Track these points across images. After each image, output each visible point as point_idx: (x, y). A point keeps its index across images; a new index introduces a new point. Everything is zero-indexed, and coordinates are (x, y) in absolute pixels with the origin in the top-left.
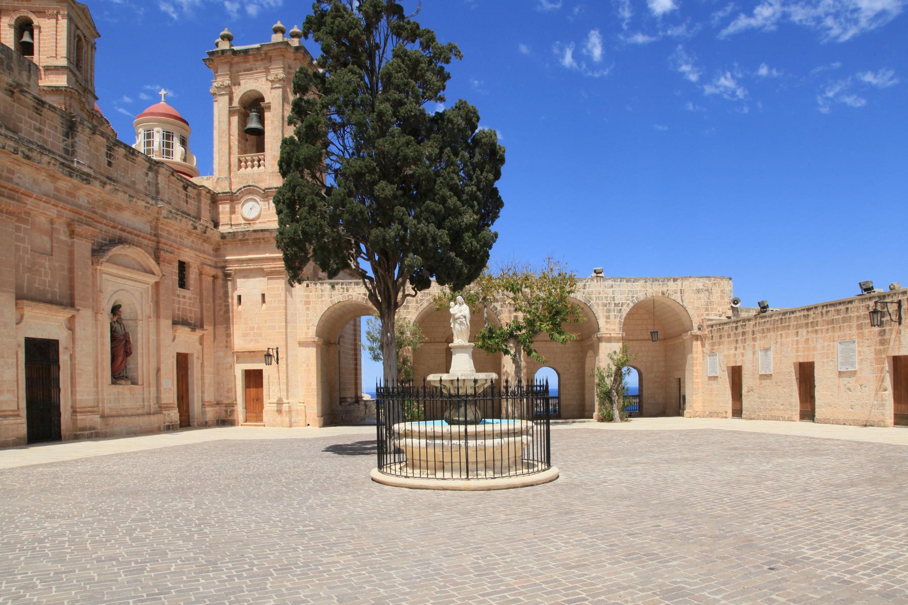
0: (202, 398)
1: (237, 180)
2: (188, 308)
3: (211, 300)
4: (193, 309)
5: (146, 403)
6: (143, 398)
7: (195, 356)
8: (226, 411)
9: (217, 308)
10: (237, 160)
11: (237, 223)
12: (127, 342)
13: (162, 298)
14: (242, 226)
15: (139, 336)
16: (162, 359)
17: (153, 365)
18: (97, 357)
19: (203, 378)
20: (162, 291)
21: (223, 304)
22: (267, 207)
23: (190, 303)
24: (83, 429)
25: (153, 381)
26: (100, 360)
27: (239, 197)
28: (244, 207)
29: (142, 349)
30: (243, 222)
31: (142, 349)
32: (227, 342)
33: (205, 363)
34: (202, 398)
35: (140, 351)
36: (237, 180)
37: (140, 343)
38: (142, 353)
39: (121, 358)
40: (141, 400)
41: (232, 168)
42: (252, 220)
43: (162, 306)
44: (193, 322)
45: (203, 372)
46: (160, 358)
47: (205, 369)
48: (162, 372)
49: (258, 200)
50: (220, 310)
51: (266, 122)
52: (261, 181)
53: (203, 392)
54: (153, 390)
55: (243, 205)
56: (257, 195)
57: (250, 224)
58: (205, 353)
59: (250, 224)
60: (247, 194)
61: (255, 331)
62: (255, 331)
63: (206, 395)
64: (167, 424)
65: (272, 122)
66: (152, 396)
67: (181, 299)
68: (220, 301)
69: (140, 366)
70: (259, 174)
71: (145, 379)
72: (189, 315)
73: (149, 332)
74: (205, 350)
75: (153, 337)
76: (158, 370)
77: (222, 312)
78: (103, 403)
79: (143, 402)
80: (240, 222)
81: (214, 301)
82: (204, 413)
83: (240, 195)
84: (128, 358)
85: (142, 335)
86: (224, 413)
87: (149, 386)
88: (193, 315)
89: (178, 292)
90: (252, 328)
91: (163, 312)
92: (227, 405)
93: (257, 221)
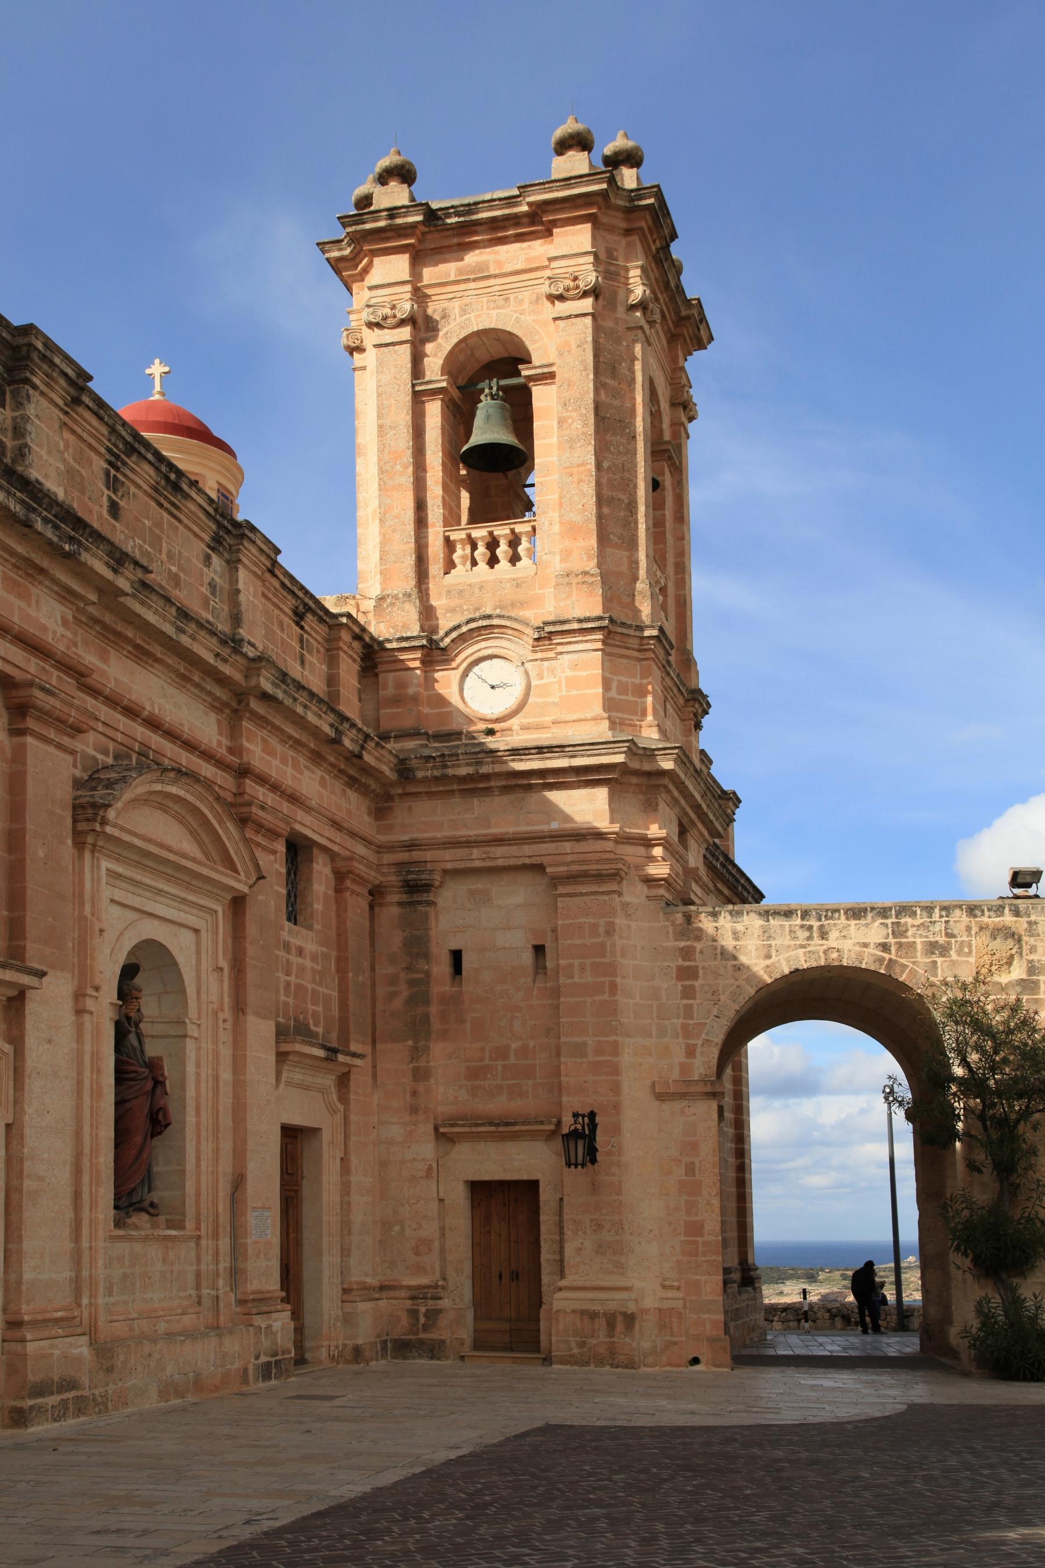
0: (344, 1270)
2: (310, 986)
3: (366, 964)
4: (322, 990)
5: (205, 1292)
6: (198, 1274)
7: (326, 1135)
8: (413, 1313)
9: (381, 991)
12: (158, 1083)
13: (251, 950)
15: (191, 1068)
16: (251, 1145)
17: (226, 1165)
18: (78, 1134)
19: (346, 1208)
20: (252, 930)
21: (403, 976)
23: (314, 971)
24: (41, 1390)
25: (224, 1218)
26: (87, 1150)
29: (198, 1114)
31: (198, 1114)
32: (414, 1093)
33: (354, 1160)
34: (344, 1270)
35: (190, 1118)
37: (191, 1092)
38: (198, 1124)
39: (138, 1139)
40: (191, 1278)
43: (251, 976)
44: (320, 1030)
45: (346, 1189)
46: (244, 1142)
47: (353, 1179)
48: (251, 1187)
50: (392, 996)
51: (537, 425)
52: (523, 604)
53: (345, 1252)
54: (224, 1244)
58: (353, 1128)
61: (512, 1060)
62: (512, 1060)
63: (353, 1261)
64: (263, 1359)
65: (561, 422)
66: (221, 1267)
67: (294, 959)
68: (390, 970)
69: (190, 1166)
70: (518, 584)
71: (204, 1211)
72: (311, 1007)
73: (216, 1054)
74: (353, 1118)
75: (226, 1075)
76: (238, 1182)
77: (398, 1003)
78: (93, 1296)
79: (198, 1286)
81: (373, 969)
82: (348, 1319)
84: (156, 1142)
85: (198, 1065)
86: (405, 1320)
87: (216, 1236)
88: (320, 1009)
89: (285, 935)
90: (502, 1053)
91: (253, 997)
92: (418, 1294)
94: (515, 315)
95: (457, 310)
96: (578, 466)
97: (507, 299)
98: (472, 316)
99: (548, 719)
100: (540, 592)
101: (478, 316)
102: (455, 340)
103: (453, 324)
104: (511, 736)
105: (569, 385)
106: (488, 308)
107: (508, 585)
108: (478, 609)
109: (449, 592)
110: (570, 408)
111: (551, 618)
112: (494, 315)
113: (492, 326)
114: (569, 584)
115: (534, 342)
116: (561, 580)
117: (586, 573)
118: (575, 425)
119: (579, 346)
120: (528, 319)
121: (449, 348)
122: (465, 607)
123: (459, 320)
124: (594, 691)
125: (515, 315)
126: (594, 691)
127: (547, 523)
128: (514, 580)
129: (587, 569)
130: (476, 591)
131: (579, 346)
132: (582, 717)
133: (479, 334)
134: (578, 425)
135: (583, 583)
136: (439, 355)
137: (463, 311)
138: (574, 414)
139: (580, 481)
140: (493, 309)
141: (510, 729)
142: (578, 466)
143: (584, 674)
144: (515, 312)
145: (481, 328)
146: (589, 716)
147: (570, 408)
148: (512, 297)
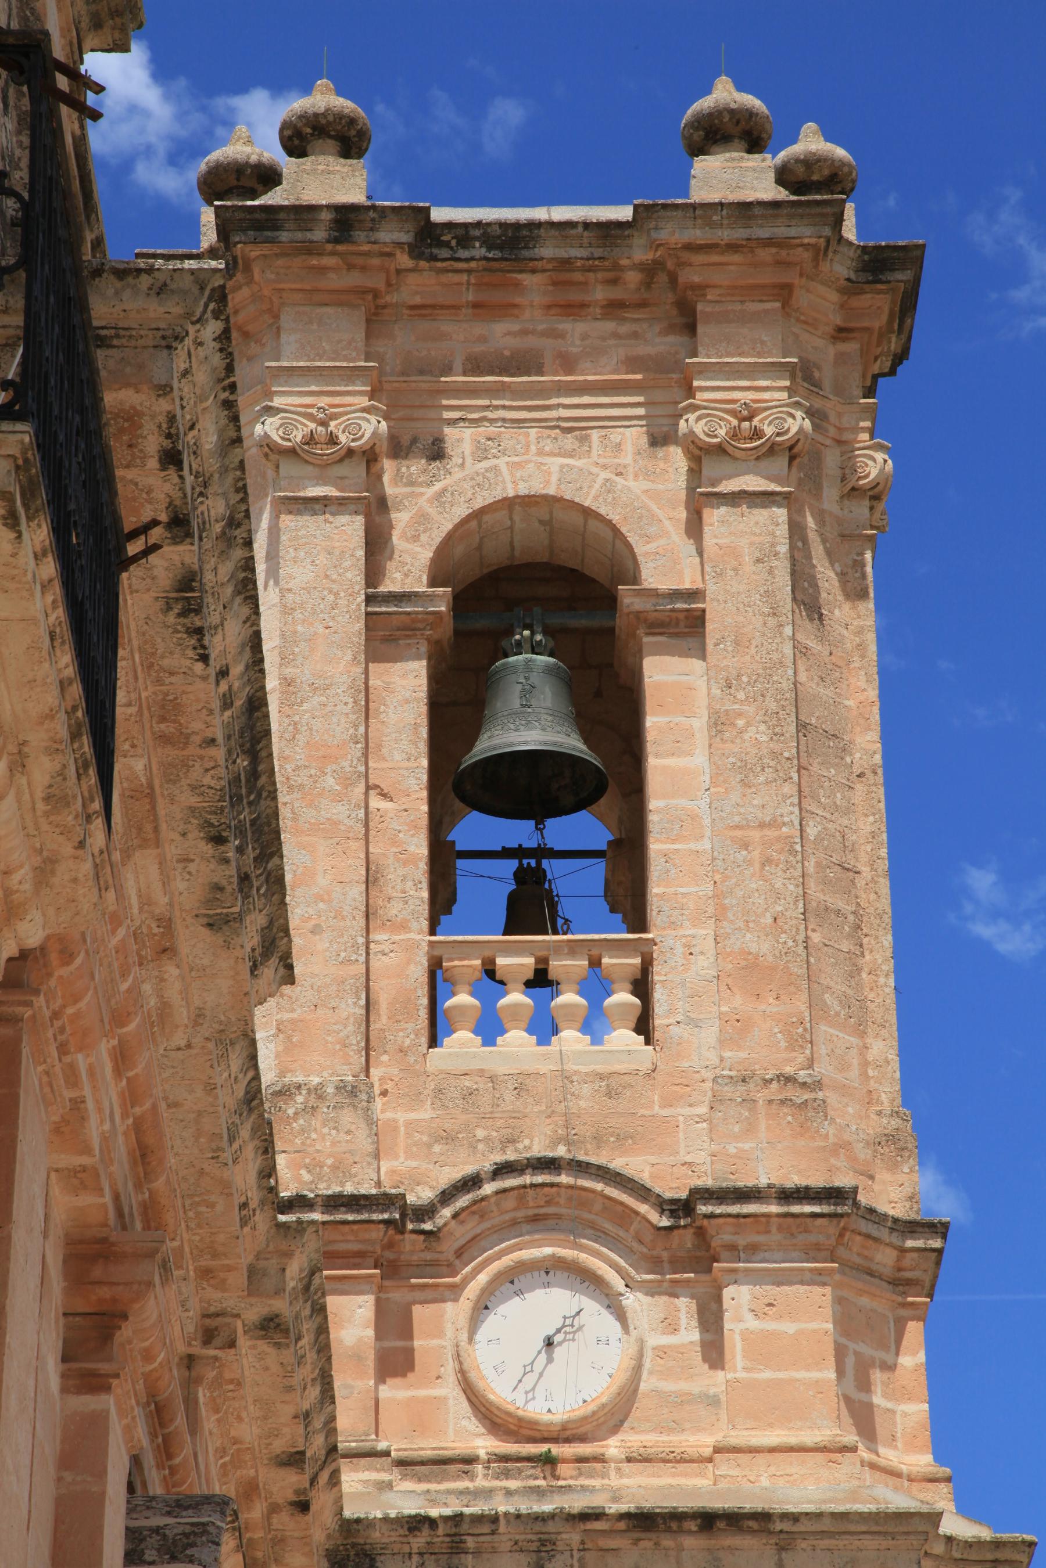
1: (425, 1113)
10: (419, 972)
11: (427, 1446)
14: (481, 1480)
22: (690, 1334)
27: (448, 1248)
28: (492, 1324)
30: (484, 1444)
36: (425, 1113)
41: (381, 1021)
42: (566, 1434)
49: (617, 1283)
51: (653, 722)
52: (623, 1140)
55: (483, 1307)
56: (601, 1236)
57: (549, 1461)
59: (549, 1461)
60: (512, 1227)
65: (719, 723)
80: (454, 1444)
83: (461, 1233)
93: (613, 1447)
94: (604, 475)
95: (467, 447)
96: (762, 826)
97: (585, 440)
98: (502, 462)
99: (702, 1442)
100: (665, 1112)
101: (519, 465)
102: (461, 511)
103: (458, 475)
104: (603, 1476)
105: (737, 643)
106: (541, 453)
107: (586, 1089)
108: (513, 1141)
109: (439, 1092)
110: (741, 695)
111: (709, 1182)
112: (555, 469)
113: (551, 491)
114: (749, 1101)
115: (649, 538)
116: (728, 1091)
117: (789, 1079)
118: (751, 732)
119: (758, 561)
120: (636, 486)
121: (449, 526)
122: (480, 1133)
123: (471, 467)
124: (815, 1375)
125: (604, 475)
126: (815, 1375)
127: (679, 949)
128: (601, 1077)
129: (789, 1070)
130: (509, 1096)
131: (758, 561)
132: (793, 1441)
133: (509, 504)
134: (759, 733)
135: (782, 1102)
136: (424, 538)
137: (481, 453)
138: (750, 709)
139: (767, 861)
140: (552, 454)
141: (600, 1459)
142: (762, 826)
143: (790, 1327)
144: (605, 467)
145: (523, 490)
146: (809, 1438)
147: (741, 695)
148: (595, 435)
